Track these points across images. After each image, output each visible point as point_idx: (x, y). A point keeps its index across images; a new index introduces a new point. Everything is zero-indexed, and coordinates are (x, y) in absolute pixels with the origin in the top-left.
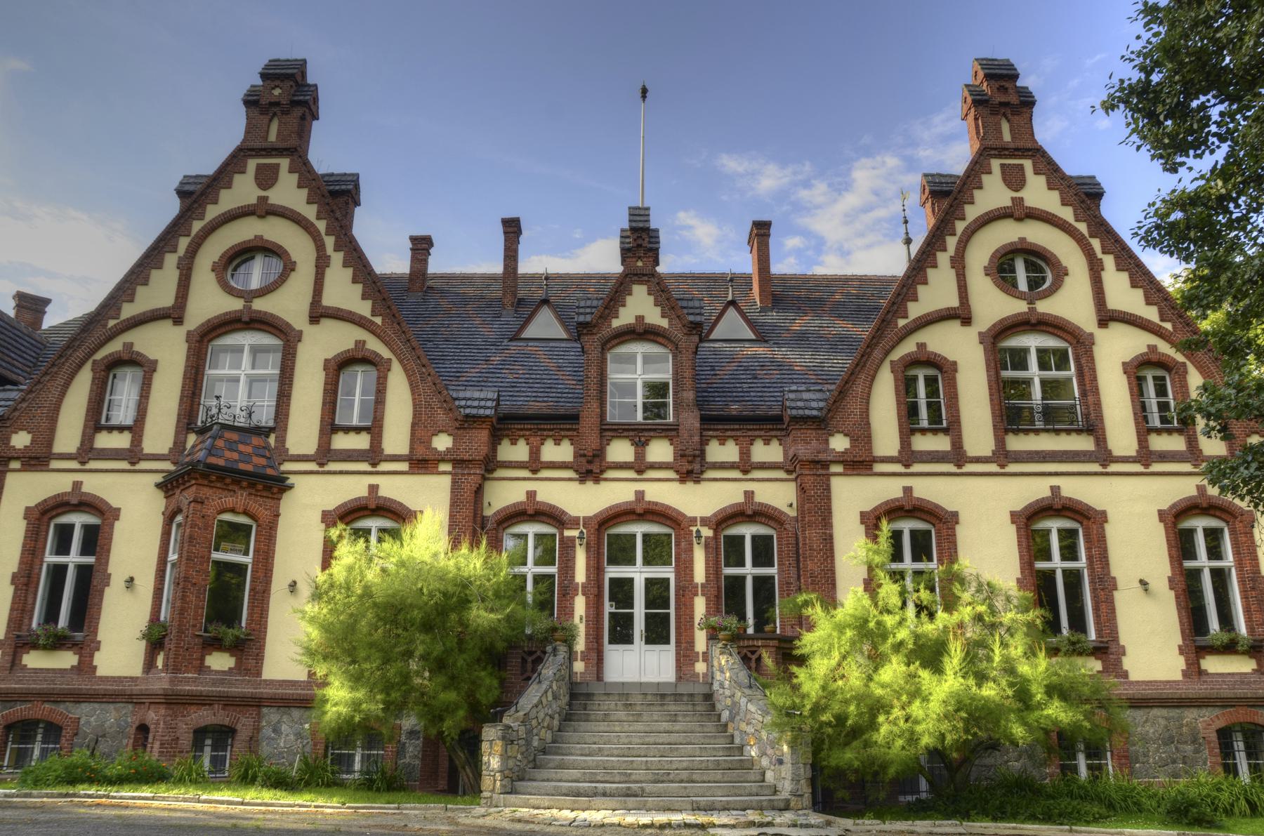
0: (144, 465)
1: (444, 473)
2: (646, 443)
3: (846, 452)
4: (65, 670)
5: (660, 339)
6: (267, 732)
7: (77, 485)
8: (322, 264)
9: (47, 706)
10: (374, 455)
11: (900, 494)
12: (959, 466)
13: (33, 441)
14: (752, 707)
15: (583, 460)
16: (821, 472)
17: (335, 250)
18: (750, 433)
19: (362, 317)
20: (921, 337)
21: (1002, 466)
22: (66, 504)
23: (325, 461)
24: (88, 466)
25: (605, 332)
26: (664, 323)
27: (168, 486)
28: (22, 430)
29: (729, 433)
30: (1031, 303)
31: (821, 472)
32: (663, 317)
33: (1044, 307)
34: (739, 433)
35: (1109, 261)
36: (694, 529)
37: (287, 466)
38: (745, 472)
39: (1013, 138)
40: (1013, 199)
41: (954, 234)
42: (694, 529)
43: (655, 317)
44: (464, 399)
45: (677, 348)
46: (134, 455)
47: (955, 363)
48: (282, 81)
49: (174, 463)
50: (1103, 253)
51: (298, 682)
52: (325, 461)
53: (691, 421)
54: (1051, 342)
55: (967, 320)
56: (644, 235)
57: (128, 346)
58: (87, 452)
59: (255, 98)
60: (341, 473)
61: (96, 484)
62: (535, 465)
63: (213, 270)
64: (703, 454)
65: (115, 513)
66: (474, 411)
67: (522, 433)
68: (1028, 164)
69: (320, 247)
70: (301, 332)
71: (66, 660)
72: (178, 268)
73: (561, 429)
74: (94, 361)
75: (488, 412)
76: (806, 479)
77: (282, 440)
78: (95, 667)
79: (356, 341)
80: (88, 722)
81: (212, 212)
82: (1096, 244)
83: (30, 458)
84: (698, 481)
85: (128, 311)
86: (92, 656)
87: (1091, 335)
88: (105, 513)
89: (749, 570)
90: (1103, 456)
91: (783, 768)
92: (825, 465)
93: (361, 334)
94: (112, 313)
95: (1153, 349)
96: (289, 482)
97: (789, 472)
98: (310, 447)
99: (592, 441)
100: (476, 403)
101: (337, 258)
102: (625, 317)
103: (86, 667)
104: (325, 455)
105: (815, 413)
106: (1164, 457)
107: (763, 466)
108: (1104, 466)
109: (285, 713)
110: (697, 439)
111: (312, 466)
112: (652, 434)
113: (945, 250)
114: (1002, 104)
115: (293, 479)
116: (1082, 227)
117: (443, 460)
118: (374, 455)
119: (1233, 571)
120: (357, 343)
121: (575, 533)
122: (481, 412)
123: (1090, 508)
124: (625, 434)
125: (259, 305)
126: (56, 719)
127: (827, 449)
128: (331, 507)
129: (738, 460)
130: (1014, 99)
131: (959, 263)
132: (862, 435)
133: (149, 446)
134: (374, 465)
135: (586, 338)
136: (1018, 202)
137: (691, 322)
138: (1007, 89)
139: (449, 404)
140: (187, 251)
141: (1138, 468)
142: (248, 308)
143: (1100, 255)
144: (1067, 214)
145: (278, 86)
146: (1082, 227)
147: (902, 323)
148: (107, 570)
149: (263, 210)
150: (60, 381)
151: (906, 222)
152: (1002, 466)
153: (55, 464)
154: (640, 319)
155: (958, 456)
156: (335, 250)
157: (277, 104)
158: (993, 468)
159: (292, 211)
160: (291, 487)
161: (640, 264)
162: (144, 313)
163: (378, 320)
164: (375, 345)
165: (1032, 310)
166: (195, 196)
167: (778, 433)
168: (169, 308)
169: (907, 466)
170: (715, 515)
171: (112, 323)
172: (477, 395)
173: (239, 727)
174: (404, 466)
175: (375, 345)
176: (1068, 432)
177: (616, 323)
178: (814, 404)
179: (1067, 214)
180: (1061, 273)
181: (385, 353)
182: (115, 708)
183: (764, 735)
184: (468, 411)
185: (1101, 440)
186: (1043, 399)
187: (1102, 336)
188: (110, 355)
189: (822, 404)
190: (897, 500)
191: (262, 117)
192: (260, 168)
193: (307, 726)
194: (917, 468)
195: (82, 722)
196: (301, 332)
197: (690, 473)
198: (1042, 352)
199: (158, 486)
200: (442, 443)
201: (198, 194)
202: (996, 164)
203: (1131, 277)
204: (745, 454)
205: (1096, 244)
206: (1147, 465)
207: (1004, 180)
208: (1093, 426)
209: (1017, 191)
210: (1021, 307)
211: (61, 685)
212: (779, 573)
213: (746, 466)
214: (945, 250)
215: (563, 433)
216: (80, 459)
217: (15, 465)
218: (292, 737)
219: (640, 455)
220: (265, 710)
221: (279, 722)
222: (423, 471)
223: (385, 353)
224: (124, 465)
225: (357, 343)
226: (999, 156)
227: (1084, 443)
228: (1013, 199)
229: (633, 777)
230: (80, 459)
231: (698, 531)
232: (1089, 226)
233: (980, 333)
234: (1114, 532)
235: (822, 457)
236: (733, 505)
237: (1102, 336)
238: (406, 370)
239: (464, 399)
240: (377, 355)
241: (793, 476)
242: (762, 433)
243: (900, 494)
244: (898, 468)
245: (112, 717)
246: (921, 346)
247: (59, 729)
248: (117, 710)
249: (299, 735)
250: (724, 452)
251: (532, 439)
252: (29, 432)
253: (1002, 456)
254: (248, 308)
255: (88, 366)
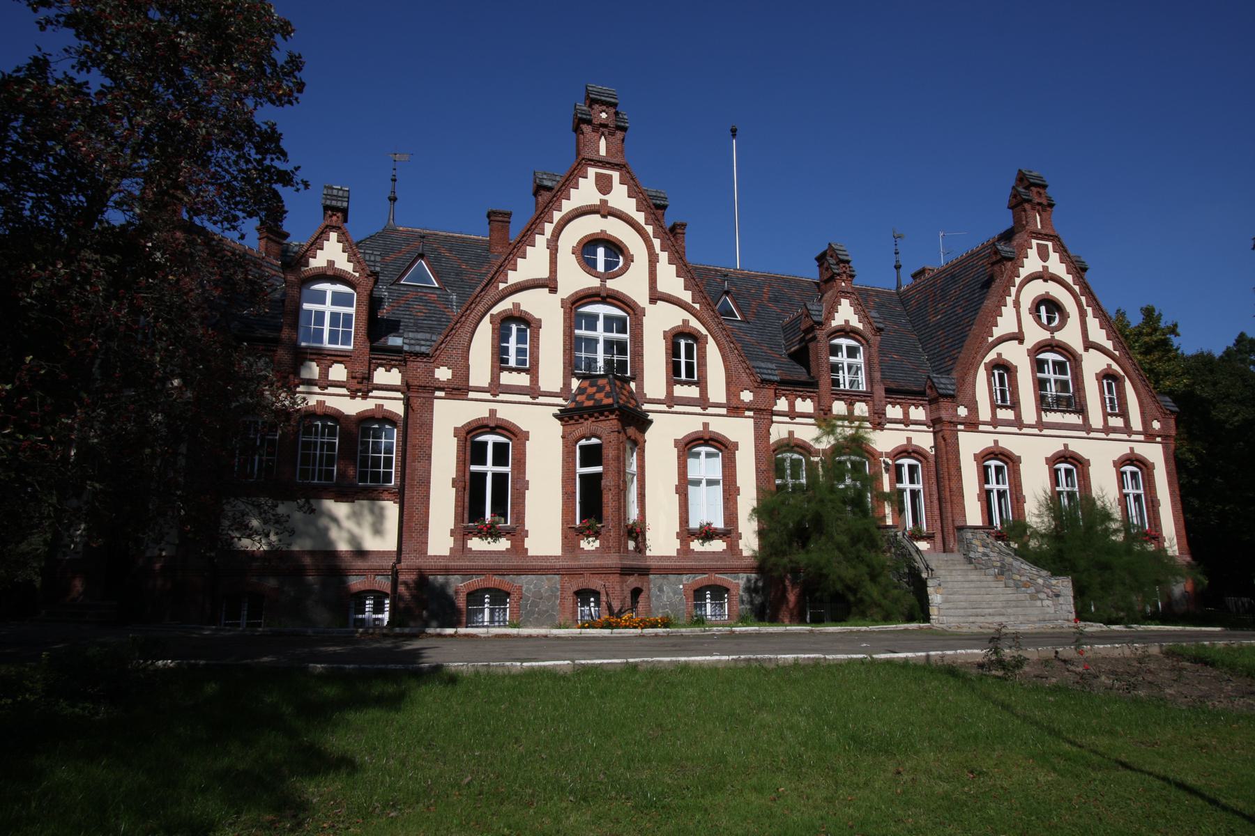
0: (541, 399)
1: (749, 417)
2: (853, 405)
3: (966, 417)
4: (503, 551)
5: (857, 337)
6: (654, 591)
7: (493, 412)
8: (653, 260)
9: (496, 577)
10: (703, 402)
11: (992, 444)
12: (1020, 429)
13: (453, 375)
14: (1023, 566)
15: (822, 412)
16: (953, 428)
17: (662, 250)
18: (909, 401)
19: (686, 303)
20: (999, 349)
21: (1041, 431)
22: (486, 426)
23: (672, 404)
24: (498, 398)
25: (827, 330)
26: (860, 326)
27: (565, 416)
28: (443, 366)
29: (898, 401)
30: (1052, 333)
31: (953, 428)
32: (860, 322)
33: (1059, 336)
34: (903, 401)
35: (1089, 310)
36: (882, 459)
37: (646, 407)
38: (907, 425)
39: (1042, 227)
40: (1043, 267)
41: (1014, 286)
42: (882, 459)
43: (855, 322)
44: (758, 367)
45: (867, 341)
46: (533, 391)
47: (1016, 367)
48: (607, 107)
49: (566, 400)
50: (1087, 306)
51: (670, 557)
52: (672, 404)
53: (880, 391)
54: (1059, 358)
55: (1021, 341)
56: (847, 265)
57: (517, 305)
58: (496, 388)
59: (588, 117)
60: (684, 413)
61: (506, 413)
62: (792, 414)
63: (573, 253)
64: (885, 414)
65: (526, 436)
66: (767, 377)
67: (784, 392)
68: (1050, 244)
69: (650, 247)
70: (644, 309)
71: (503, 544)
72: (548, 248)
73: (808, 392)
74: (492, 315)
75: (776, 378)
76: (946, 432)
77: (640, 386)
78: (527, 549)
79: (683, 320)
80: (528, 589)
81: (567, 206)
82: (1083, 299)
83: (453, 389)
84: (882, 429)
85: (513, 278)
86: (523, 541)
87: (1081, 355)
88: (517, 435)
89: (906, 485)
90: (1086, 427)
91: (1061, 600)
92: (956, 424)
93: (687, 316)
94: (501, 277)
95: (1109, 366)
96: (649, 418)
97: (929, 427)
98: (661, 394)
99: (824, 402)
100: (765, 371)
101: (663, 257)
102: (838, 321)
103: (518, 548)
104: (671, 400)
105: (952, 392)
106: (1115, 430)
107: (916, 423)
108: (1088, 433)
109: (664, 578)
110: (884, 403)
111: (664, 408)
112: (857, 398)
113: (1010, 296)
114: (1039, 204)
115: (651, 416)
116: (1077, 288)
117: (749, 410)
118: (703, 402)
119: (1143, 496)
120: (684, 321)
121: (816, 459)
122: (772, 377)
123: (1083, 458)
124: (843, 397)
125: (611, 284)
126: (505, 588)
127: (957, 416)
128: (680, 437)
129: (902, 417)
130: (1045, 202)
131: (1017, 304)
132: (973, 408)
133: (544, 386)
134: (704, 409)
135: (818, 332)
136: (1045, 268)
137: (878, 328)
138: (1040, 194)
139: (751, 371)
140: (552, 235)
141: (1103, 435)
142: (603, 285)
143: (1085, 307)
144: (1069, 279)
145: (604, 111)
146: (1077, 288)
147: (990, 339)
148: (525, 478)
149: (604, 211)
150: (468, 328)
151: (897, 253)
152: (1041, 431)
153: (471, 395)
154: (847, 322)
155: (1018, 422)
156: (662, 250)
157: (605, 126)
158: (1036, 431)
159: (627, 215)
160: (651, 422)
161: (843, 284)
162: (527, 281)
163: (697, 306)
164: (695, 324)
165: (1053, 337)
166: (554, 191)
167: (924, 402)
168: (546, 279)
169: (995, 428)
170: (892, 451)
171: (502, 286)
172: (763, 365)
173: (644, 589)
174: (724, 411)
175: (695, 324)
176: (1070, 412)
177: (834, 324)
178: (949, 387)
179: (1069, 279)
180: (1064, 316)
181: (704, 331)
182: (547, 579)
183: (1040, 581)
184: (764, 376)
185: (1086, 419)
186: (1057, 392)
187: (1085, 355)
188: (505, 311)
189: (954, 387)
190: (991, 447)
191: (594, 134)
192: (598, 176)
193: (681, 587)
194: (1000, 429)
195: (524, 589)
196: (644, 309)
197: (879, 424)
198: (1055, 363)
199: (555, 416)
200: (747, 396)
201: (556, 188)
202: (1034, 242)
203: (1100, 322)
204: (906, 414)
205: (1083, 299)
206: (1107, 435)
207: (1039, 254)
208: (1082, 410)
209: (1045, 262)
210: (1046, 335)
211: (505, 563)
212: (924, 488)
213: (906, 421)
214: (1010, 296)
215: (808, 394)
216: (492, 392)
217: (438, 394)
218: (671, 594)
219: (851, 411)
220: (651, 576)
221: (661, 584)
222: (736, 415)
223: (704, 331)
224: (527, 399)
225: (684, 321)
226: (1036, 238)
227: (1074, 419)
228: (1043, 267)
229: (993, 606)
230: (492, 392)
231: (884, 461)
232: (1080, 288)
233: (1028, 350)
234: (1092, 470)
235: (954, 419)
236: (901, 446)
237: (1085, 355)
238: (718, 344)
239: (758, 367)
240: (699, 331)
241: (931, 429)
242: (915, 402)
243: (992, 444)
244: (990, 428)
245: (545, 584)
246: (999, 355)
247: (508, 594)
248: (548, 580)
249: (675, 593)
250: (894, 412)
251: (790, 396)
252: (449, 368)
253: (1040, 425)
254: (603, 285)
255: (487, 318)
